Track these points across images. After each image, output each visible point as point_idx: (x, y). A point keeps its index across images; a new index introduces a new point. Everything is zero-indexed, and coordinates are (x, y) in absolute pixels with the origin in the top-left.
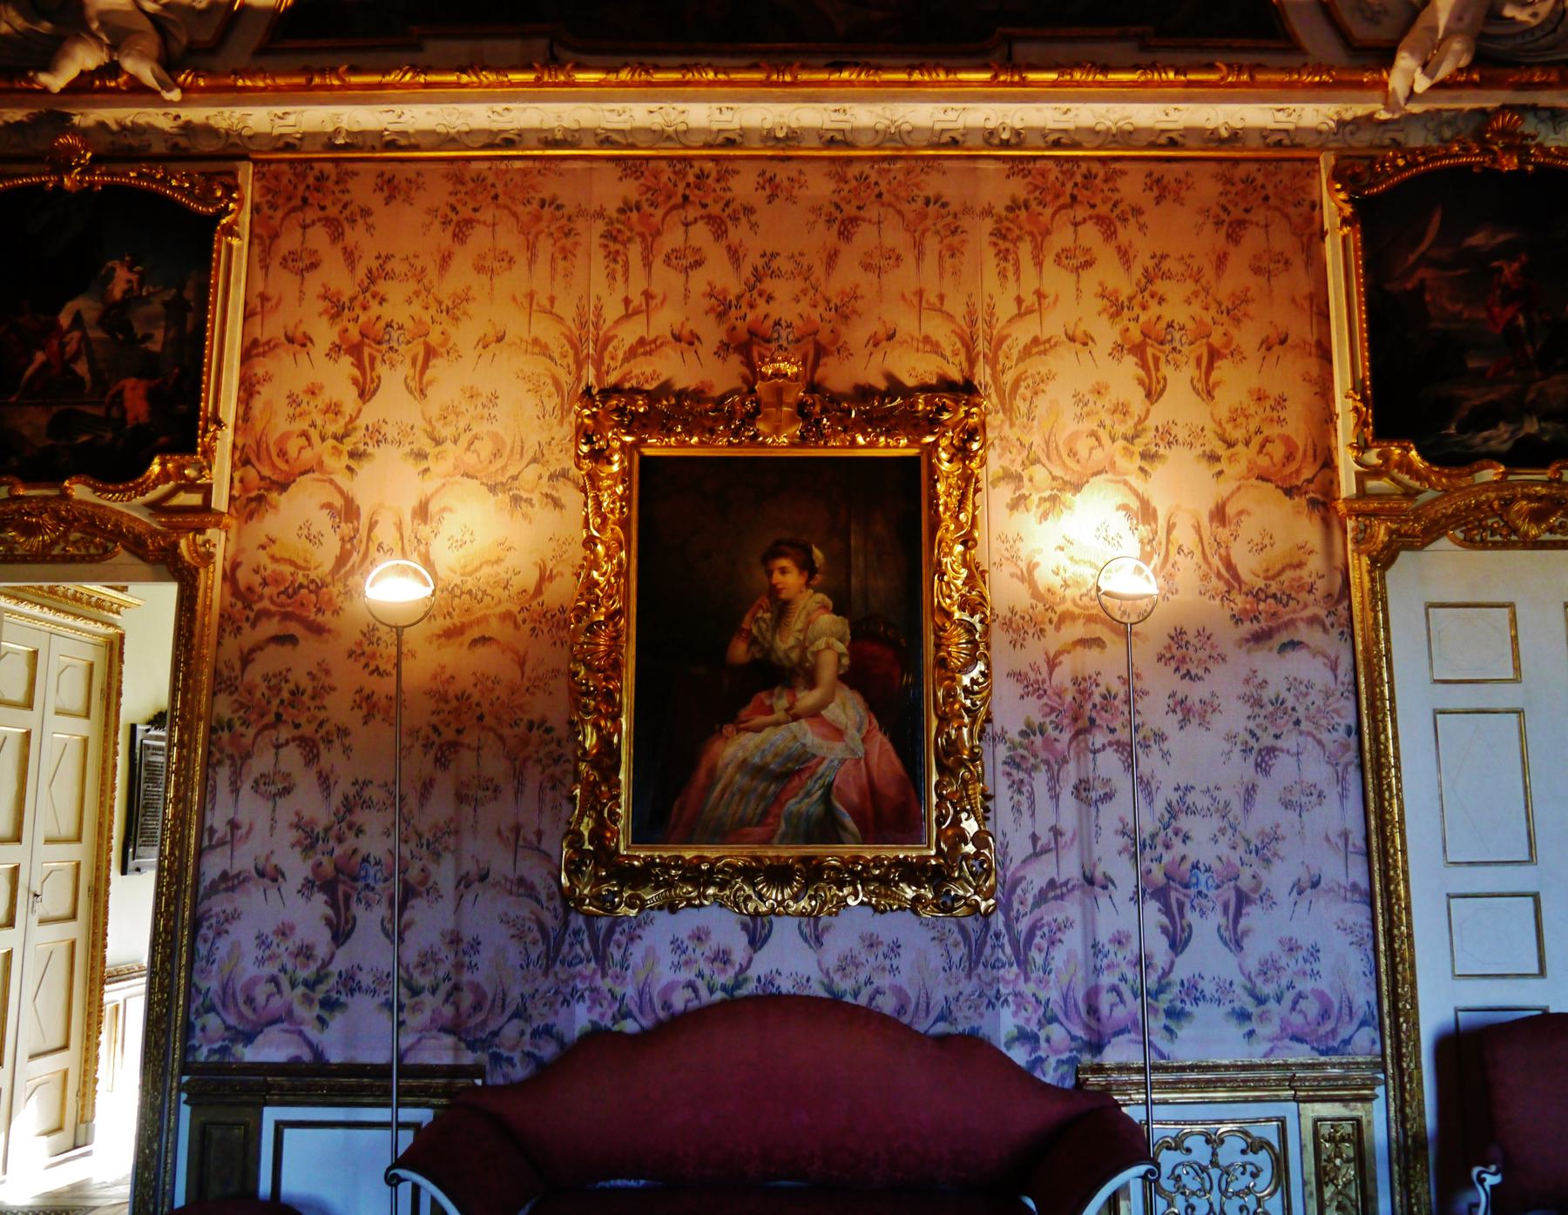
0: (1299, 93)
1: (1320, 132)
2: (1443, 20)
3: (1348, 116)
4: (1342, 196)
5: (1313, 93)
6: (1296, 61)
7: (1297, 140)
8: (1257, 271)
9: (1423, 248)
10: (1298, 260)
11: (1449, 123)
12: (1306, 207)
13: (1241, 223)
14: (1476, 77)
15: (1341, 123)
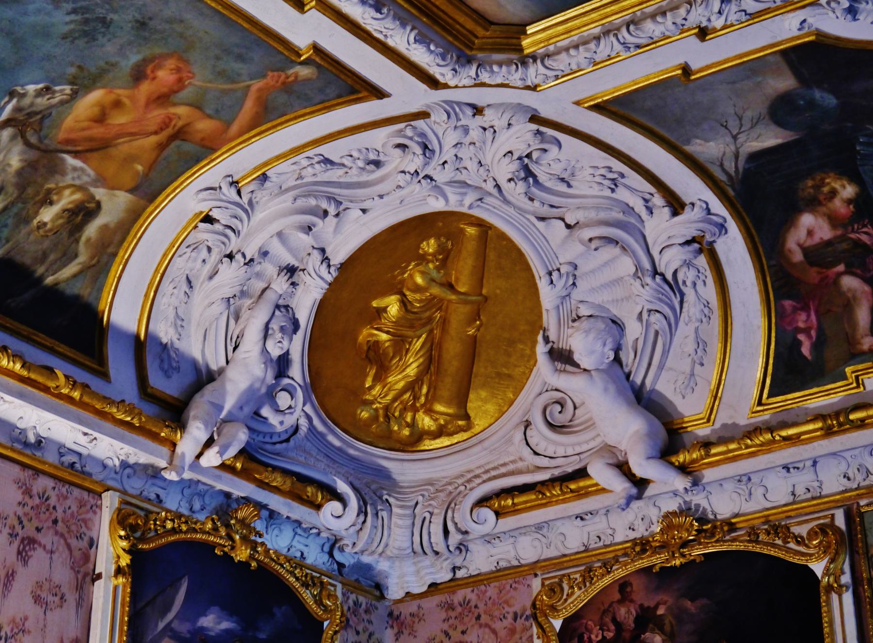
0: (108, 425)
1: (105, 466)
2: (229, 404)
3: (132, 460)
4: (124, 544)
5: (120, 430)
6: (95, 383)
7: (88, 469)
8: (37, 599)
9: (171, 616)
10: (71, 598)
11: (201, 495)
12: (84, 544)
13: (30, 542)
14: (239, 465)
15: (125, 465)
